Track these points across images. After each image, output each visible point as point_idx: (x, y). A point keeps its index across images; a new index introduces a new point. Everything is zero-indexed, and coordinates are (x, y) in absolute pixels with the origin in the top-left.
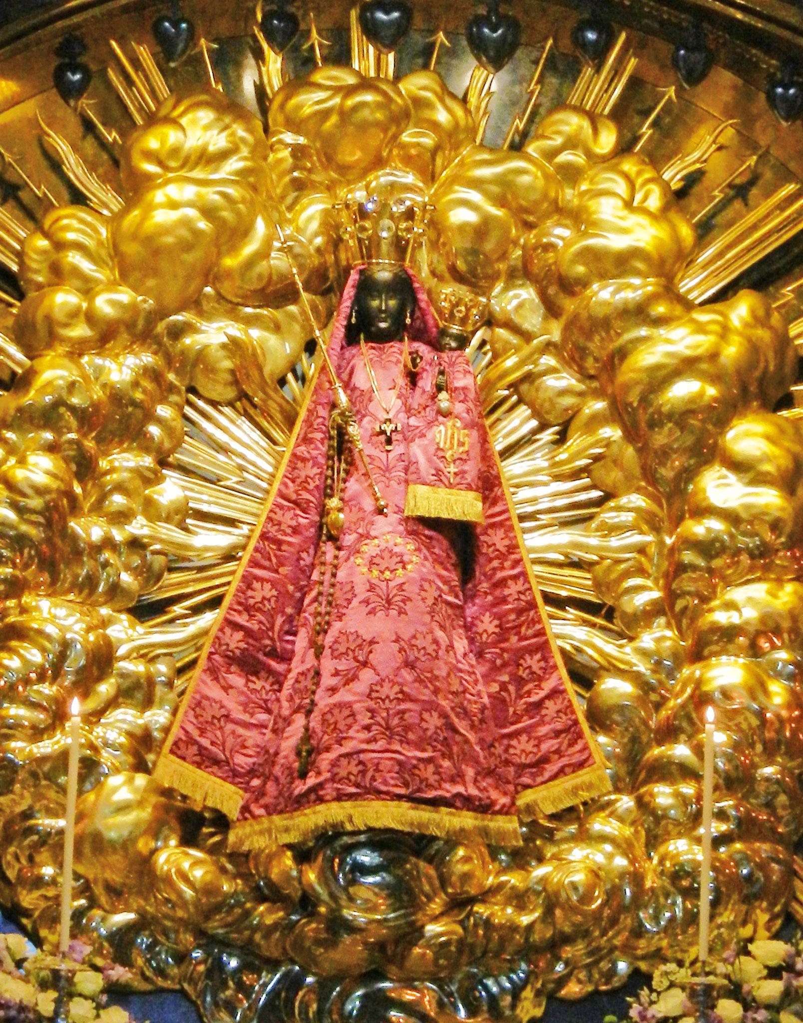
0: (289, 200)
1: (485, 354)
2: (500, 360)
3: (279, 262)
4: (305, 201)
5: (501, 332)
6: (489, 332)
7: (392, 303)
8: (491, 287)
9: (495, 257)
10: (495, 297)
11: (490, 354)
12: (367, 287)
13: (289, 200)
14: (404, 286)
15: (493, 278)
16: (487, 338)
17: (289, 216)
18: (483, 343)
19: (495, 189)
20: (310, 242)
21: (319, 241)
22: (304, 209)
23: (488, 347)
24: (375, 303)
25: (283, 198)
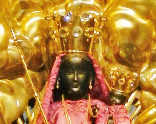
0: (19, 14)
1: (137, 107)
2: (145, 111)
3: (13, 51)
4: (28, 15)
5: (146, 94)
6: (139, 94)
7: (81, 76)
8: (141, 67)
9: (143, 48)
10: (143, 73)
11: (140, 107)
12: (66, 66)
13: (19, 14)
14: (88, 66)
15: (142, 61)
16: (138, 97)
17: (19, 24)
18: (136, 100)
19: (143, 8)
20: (32, 40)
21: (37, 39)
22: (28, 20)
23: (139, 103)
24: (71, 76)
25: (15, 13)
